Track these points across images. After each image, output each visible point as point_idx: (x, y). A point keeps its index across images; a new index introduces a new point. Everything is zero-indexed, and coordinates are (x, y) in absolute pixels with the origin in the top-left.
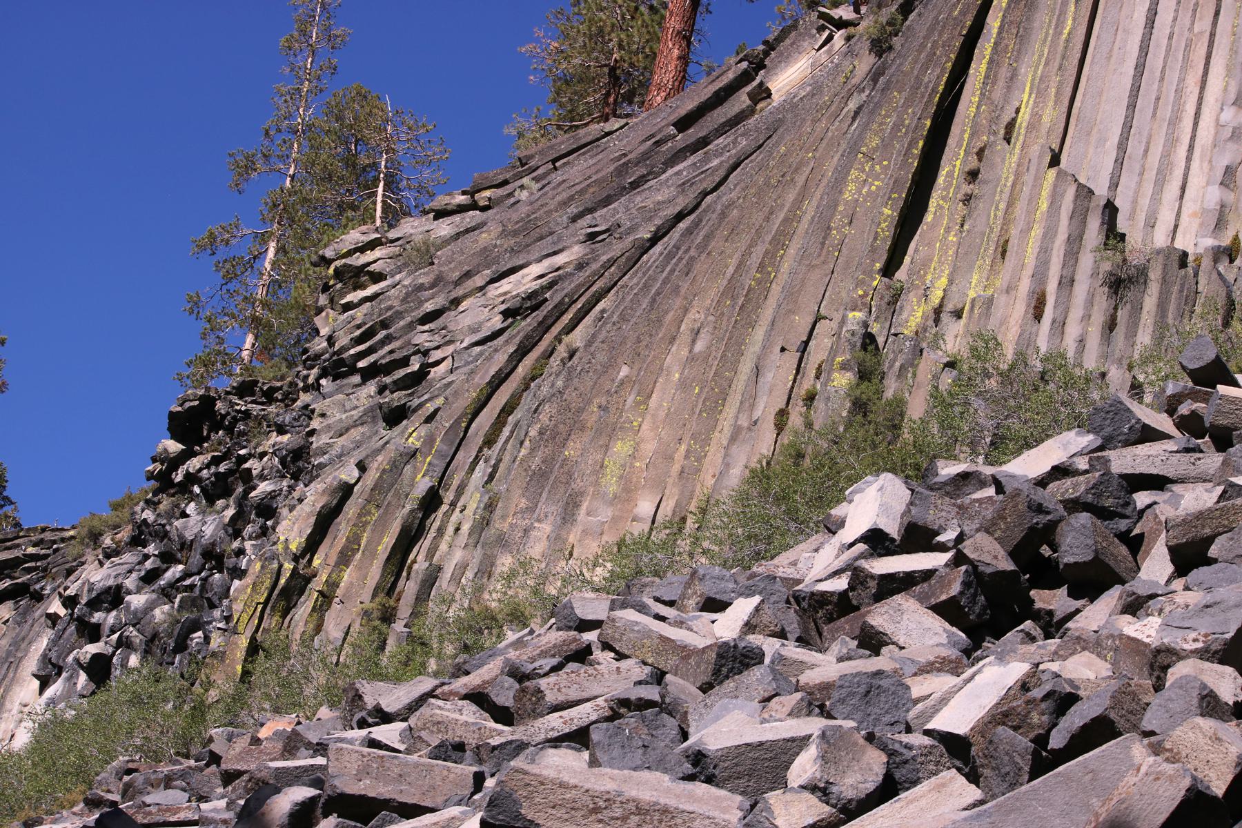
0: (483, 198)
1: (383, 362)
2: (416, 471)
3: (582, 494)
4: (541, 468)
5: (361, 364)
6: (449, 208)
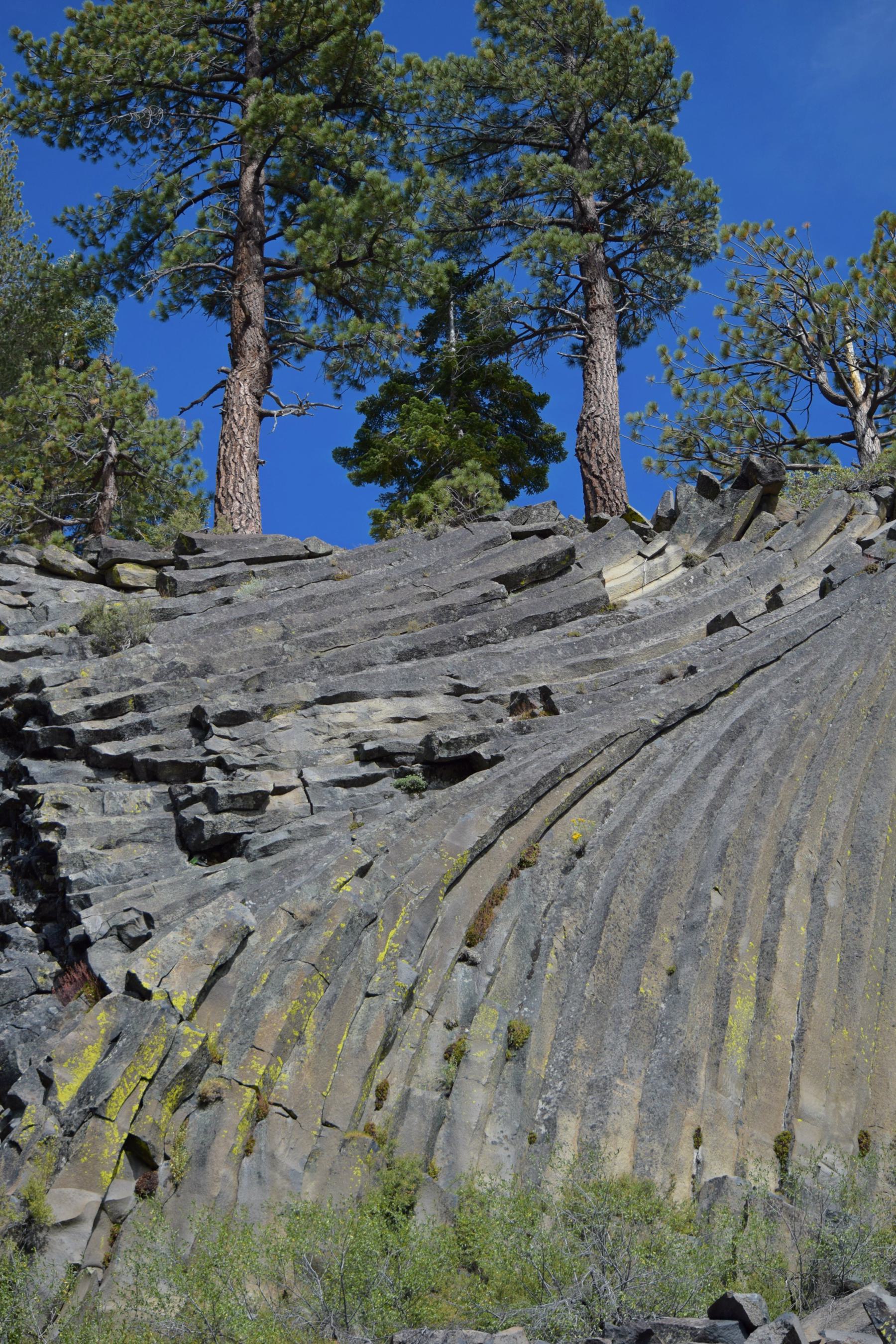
0: (127, 573)
1: (139, 757)
2: (378, 945)
3: (695, 1056)
4: (596, 1001)
5: (107, 749)
6: (67, 568)
